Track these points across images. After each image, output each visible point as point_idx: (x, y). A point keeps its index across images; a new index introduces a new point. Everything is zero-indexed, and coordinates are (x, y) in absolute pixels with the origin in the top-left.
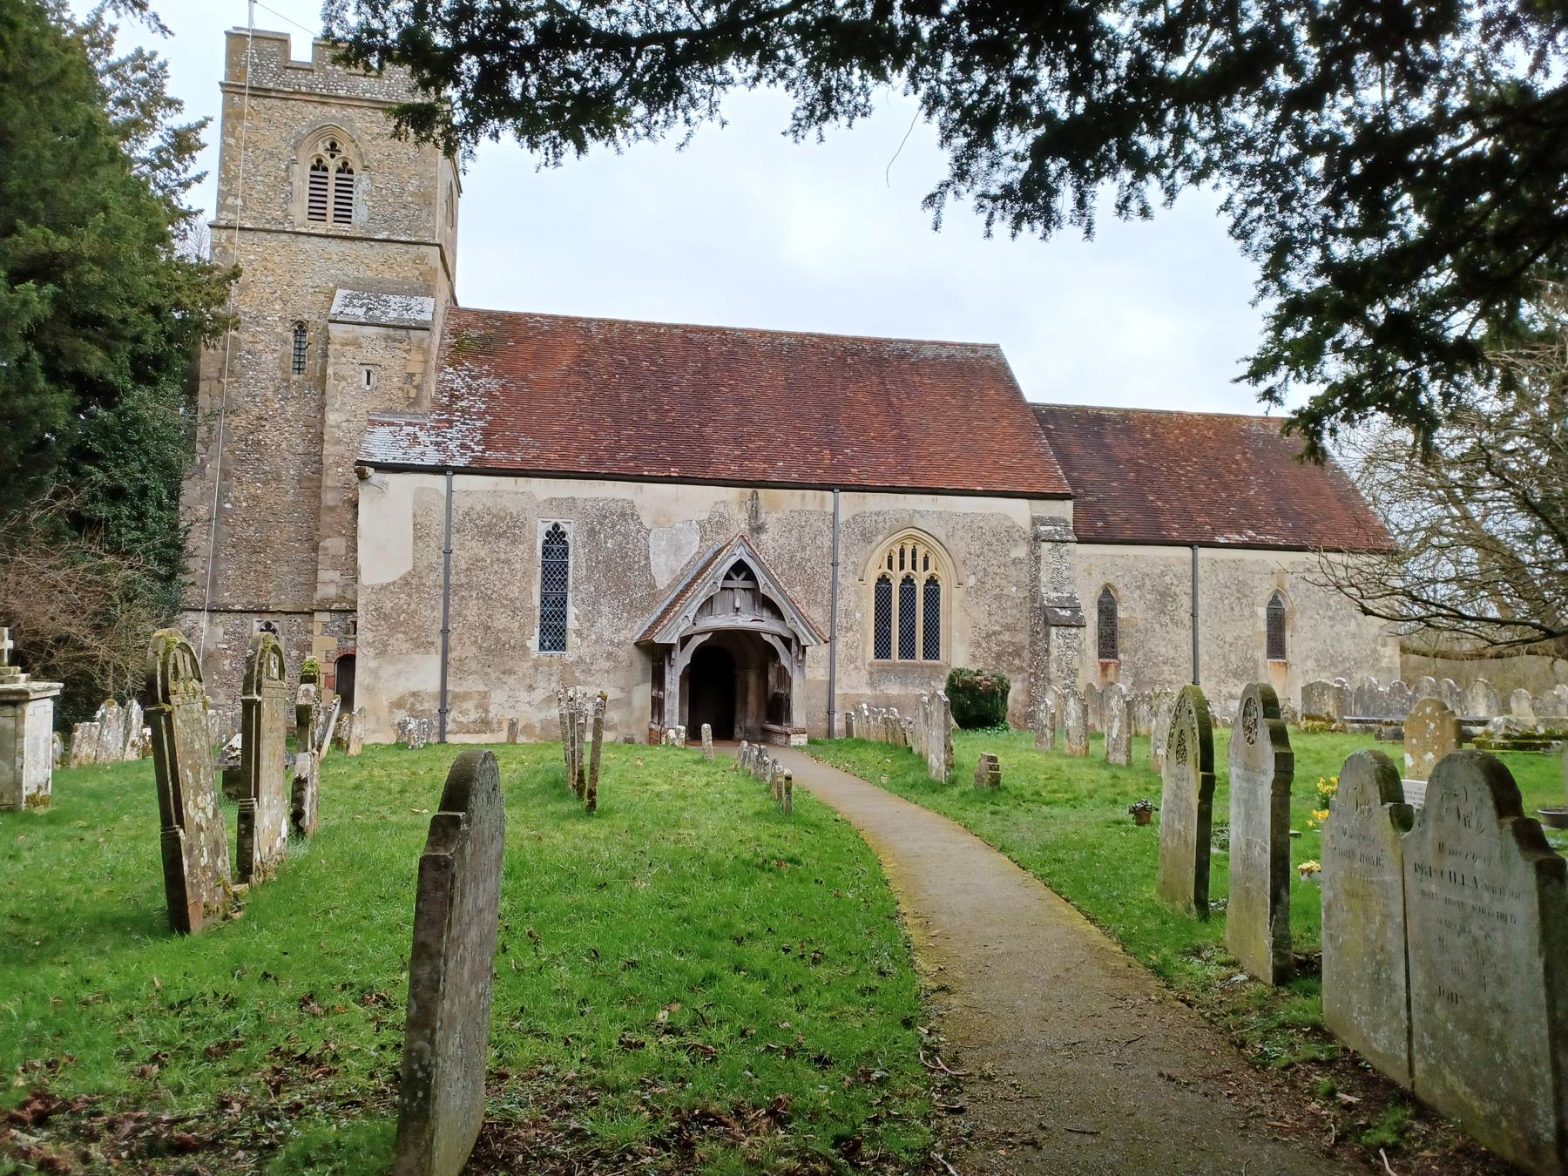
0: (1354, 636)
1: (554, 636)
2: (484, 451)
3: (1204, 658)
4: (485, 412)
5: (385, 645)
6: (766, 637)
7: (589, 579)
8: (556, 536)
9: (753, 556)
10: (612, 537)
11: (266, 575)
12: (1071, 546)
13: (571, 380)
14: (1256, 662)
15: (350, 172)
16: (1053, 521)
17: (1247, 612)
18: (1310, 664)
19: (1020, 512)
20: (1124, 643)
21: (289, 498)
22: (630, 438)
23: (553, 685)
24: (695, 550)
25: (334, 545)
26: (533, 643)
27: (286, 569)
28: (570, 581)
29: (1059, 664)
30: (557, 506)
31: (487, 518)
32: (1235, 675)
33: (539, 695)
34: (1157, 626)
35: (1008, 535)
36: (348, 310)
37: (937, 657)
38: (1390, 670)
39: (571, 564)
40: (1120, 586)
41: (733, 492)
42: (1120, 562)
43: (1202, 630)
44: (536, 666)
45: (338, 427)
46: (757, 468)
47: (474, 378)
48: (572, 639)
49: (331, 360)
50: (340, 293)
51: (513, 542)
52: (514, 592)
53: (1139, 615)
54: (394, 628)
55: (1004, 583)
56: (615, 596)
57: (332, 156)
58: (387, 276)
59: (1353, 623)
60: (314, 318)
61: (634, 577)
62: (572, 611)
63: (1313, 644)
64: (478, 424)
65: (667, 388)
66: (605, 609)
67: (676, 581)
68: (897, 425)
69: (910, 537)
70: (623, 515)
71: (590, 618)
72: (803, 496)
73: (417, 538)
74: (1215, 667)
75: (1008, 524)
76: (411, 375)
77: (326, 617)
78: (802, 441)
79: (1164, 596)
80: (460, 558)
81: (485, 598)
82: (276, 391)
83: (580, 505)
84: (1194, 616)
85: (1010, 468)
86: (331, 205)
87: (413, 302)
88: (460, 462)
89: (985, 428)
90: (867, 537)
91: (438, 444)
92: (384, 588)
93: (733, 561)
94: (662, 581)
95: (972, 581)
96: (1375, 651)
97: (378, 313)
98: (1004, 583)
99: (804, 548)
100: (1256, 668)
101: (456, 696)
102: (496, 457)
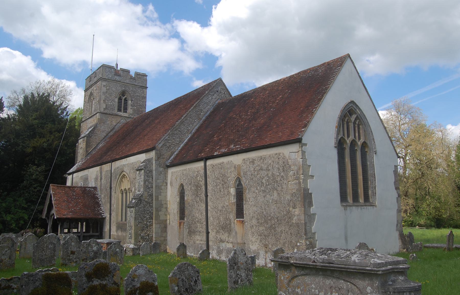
0: (276, 202)
3: (211, 219)
18: (254, 222)
20: (187, 212)
34: (195, 203)
38: (298, 225)
42: (185, 172)
43: (210, 203)
59: (275, 194)
63: (255, 208)
74: (215, 224)
79: (198, 186)
96: (289, 212)
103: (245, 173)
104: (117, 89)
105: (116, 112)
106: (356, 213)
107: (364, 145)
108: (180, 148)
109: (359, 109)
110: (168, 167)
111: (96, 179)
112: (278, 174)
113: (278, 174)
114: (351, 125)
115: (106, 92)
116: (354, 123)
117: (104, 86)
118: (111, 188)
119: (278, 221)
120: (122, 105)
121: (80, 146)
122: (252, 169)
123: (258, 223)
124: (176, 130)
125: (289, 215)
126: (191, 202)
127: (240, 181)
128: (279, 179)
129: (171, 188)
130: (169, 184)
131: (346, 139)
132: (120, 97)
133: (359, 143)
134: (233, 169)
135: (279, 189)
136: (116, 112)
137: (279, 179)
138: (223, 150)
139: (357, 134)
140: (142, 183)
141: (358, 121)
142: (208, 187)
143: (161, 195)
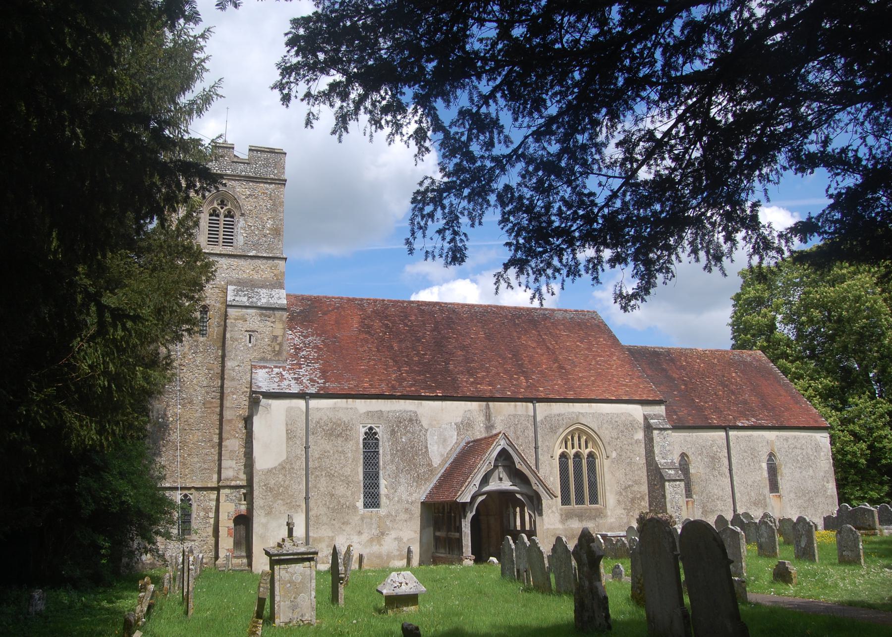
1: (372, 499)
2: (324, 383)
4: (318, 359)
5: (271, 507)
6: (518, 496)
7: (392, 461)
8: (371, 435)
9: (511, 445)
10: (405, 435)
11: (184, 464)
12: (670, 432)
13: (361, 337)
14: (764, 496)
15: (232, 217)
16: (656, 417)
17: (757, 466)
18: (792, 495)
19: (637, 412)
20: (696, 488)
21: (198, 415)
22: (407, 372)
23: (373, 531)
24: (454, 441)
25: (233, 444)
26: (360, 504)
27: (196, 460)
28: (381, 463)
29: (672, 504)
30: (372, 416)
31: (330, 425)
32: (755, 504)
33: (365, 537)
35: (630, 426)
36: (237, 298)
37: (597, 503)
39: (381, 452)
40: (689, 454)
41: (474, 405)
44: (362, 518)
45: (233, 370)
46: (485, 388)
47: (305, 337)
48: (383, 500)
49: (228, 329)
50: (231, 288)
51: (346, 440)
52: (348, 471)
53: (701, 471)
54: (276, 497)
55: (632, 455)
56: (408, 472)
57: (222, 208)
58: (256, 277)
60: (213, 303)
61: (419, 459)
62: (383, 483)
64: (317, 366)
65: (419, 340)
66: (403, 480)
67: (444, 461)
68: (556, 360)
69: (577, 429)
70: (411, 420)
71: (393, 487)
72: (516, 406)
73: (289, 438)
74: (744, 500)
75: (631, 419)
76: (276, 337)
77: (227, 491)
78: (506, 371)
79: (714, 459)
80: (314, 452)
81: (330, 476)
82: (190, 349)
83: (385, 415)
84: (730, 470)
85: (626, 386)
87: (273, 293)
88: (313, 390)
89: (604, 361)
90: (553, 429)
91: (295, 379)
92: (270, 471)
93: (499, 449)
94: (436, 461)
95: (614, 455)
96: (824, 486)
97: (254, 300)
98: (632, 455)
99: (518, 438)
100: (765, 499)
101: (315, 540)
102: (332, 386)
103: (779, 450)
135: (814, 466)
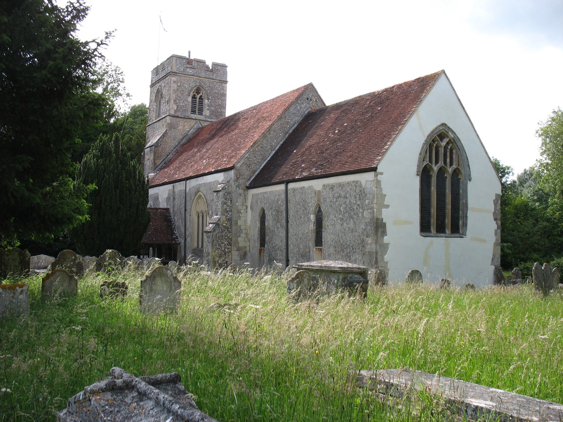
3: (291, 247)
14: (309, 248)
34: (276, 229)
42: (266, 195)
43: (290, 230)
63: (333, 236)
86: (197, 110)
96: (363, 241)
100: (309, 252)
104: (190, 84)
105: (189, 114)
106: (438, 243)
107: (456, 173)
108: (261, 168)
109: (453, 132)
110: (249, 188)
111: (168, 199)
112: (355, 202)
113: (355, 202)
114: (442, 151)
115: (177, 90)
116: (446, 148)
117: (174, 82)
118: (186, 210)
119: (353, 249)
120: (197, 105)
121: (147, 157)
122: (331, 196)
123: (335, 251)
124: (258, 146)
125: (363, 244)
126: (271, 228)
127: (320, 208)
128: (355, 208)
129: (252, 212)
130: (249, 208)
131: (433, 166)
132: (194, 95)
133: (450, 170)
134: (313, 195)
136: (189, 114)
137: (355, 208)
138: (305, 174)
139: (448, 160)
140: (220, 207)
141: (451, 145)
142: (289, 212)
143: (240, 220)
